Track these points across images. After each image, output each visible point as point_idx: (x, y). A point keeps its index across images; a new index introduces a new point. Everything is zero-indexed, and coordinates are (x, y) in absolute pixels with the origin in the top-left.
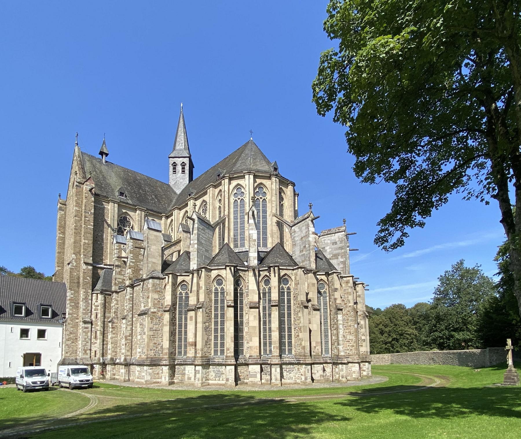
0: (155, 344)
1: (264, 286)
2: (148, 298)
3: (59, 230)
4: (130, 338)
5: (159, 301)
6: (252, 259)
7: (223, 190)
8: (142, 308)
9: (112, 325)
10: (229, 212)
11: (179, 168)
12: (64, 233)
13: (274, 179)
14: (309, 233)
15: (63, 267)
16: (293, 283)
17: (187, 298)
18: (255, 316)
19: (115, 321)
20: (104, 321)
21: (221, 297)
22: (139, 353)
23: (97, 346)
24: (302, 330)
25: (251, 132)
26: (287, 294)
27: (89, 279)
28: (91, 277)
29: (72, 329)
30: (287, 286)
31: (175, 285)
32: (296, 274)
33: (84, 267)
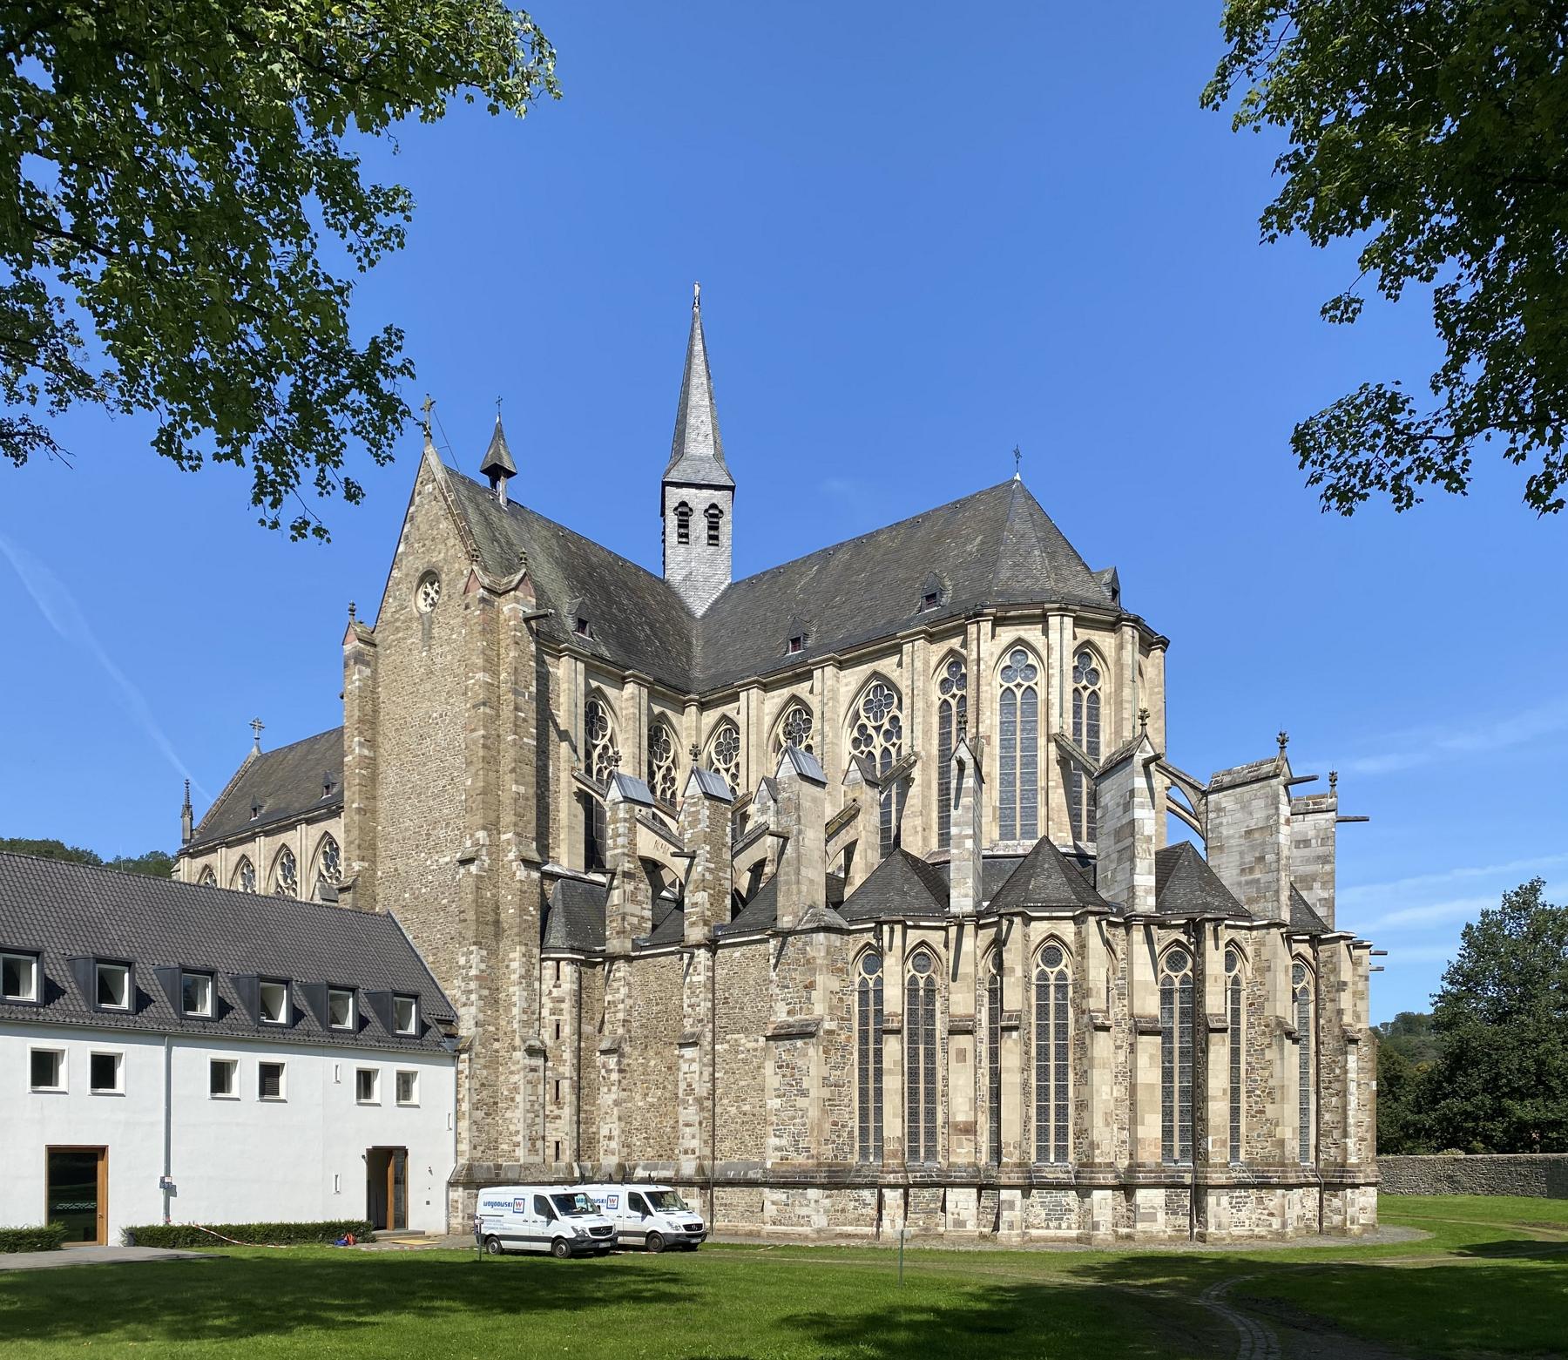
0: (835, 1124)
2: (810, 987)
3: (361, 733)
4: (708, 1104)
6: (1140, 892)
9: (619, 1063)
11: (699, 525)
12: (371, 743)
13: (1128, 632)
15: (374, 862)
16: (1249, 967)
18: (1151, 1057)
19: (627, 1049)
20: (579, 1049)
23: (562, 1129)
24: (1278, 1097)
25: (1017, 454)
29: (485, 1072)
32: (1260, 943)
33: (521, 873)
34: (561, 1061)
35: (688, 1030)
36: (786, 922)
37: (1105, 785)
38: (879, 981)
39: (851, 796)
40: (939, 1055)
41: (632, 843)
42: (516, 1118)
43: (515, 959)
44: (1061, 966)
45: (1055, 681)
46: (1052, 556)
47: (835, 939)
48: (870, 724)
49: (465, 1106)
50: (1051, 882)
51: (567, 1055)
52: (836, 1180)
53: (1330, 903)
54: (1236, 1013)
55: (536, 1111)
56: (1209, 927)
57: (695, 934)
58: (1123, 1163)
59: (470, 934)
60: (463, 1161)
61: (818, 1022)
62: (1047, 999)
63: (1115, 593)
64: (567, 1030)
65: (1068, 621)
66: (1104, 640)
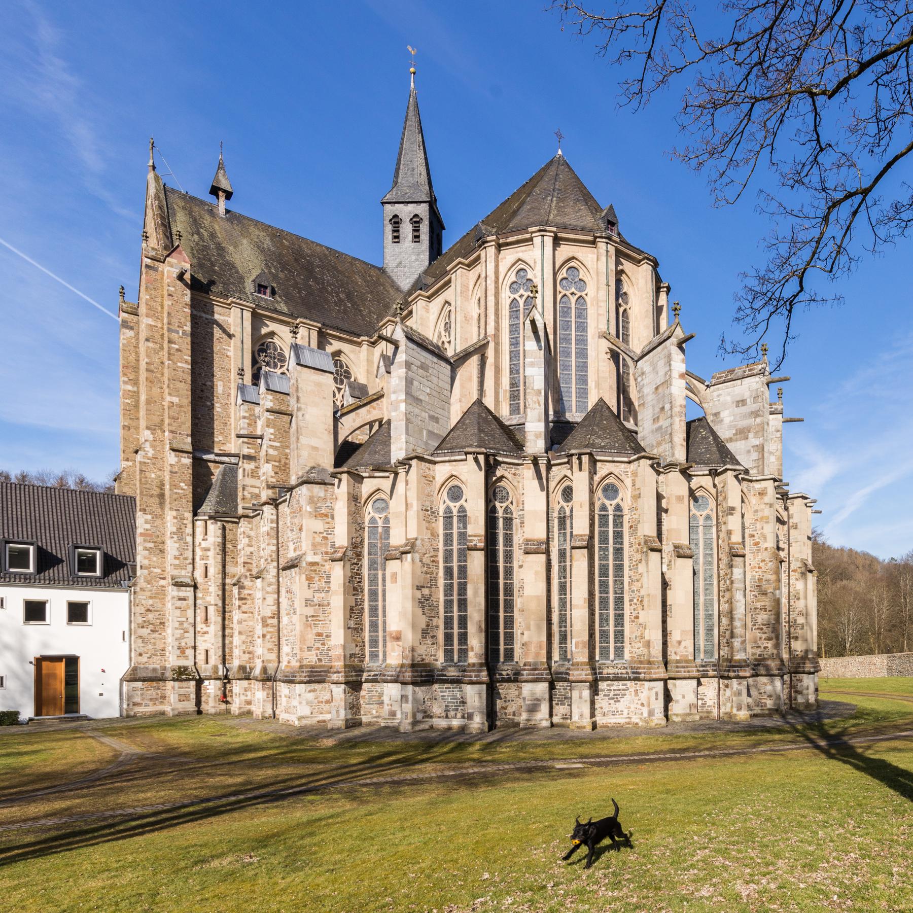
1: (562, 502)
4: (275, 621)
5: (325, 538)
7: (483, 275)
8: (292, 554)
9: (239, 593)
10: (497, 329)
14: (670, 376)
17: (387, 530)
20: (224, 585)
21: (459, 528)
22: (287, 655)
23: (209, 641)
24: (645, 603)
26: (615, 521)
27: (186, 488)
28: (190, 483)
29: (151, 602)
30: (614, 502)
31: (354, 498)
42: (170, 634)
44: (462, 502)
47: (318, 490)
62: (452, 529)
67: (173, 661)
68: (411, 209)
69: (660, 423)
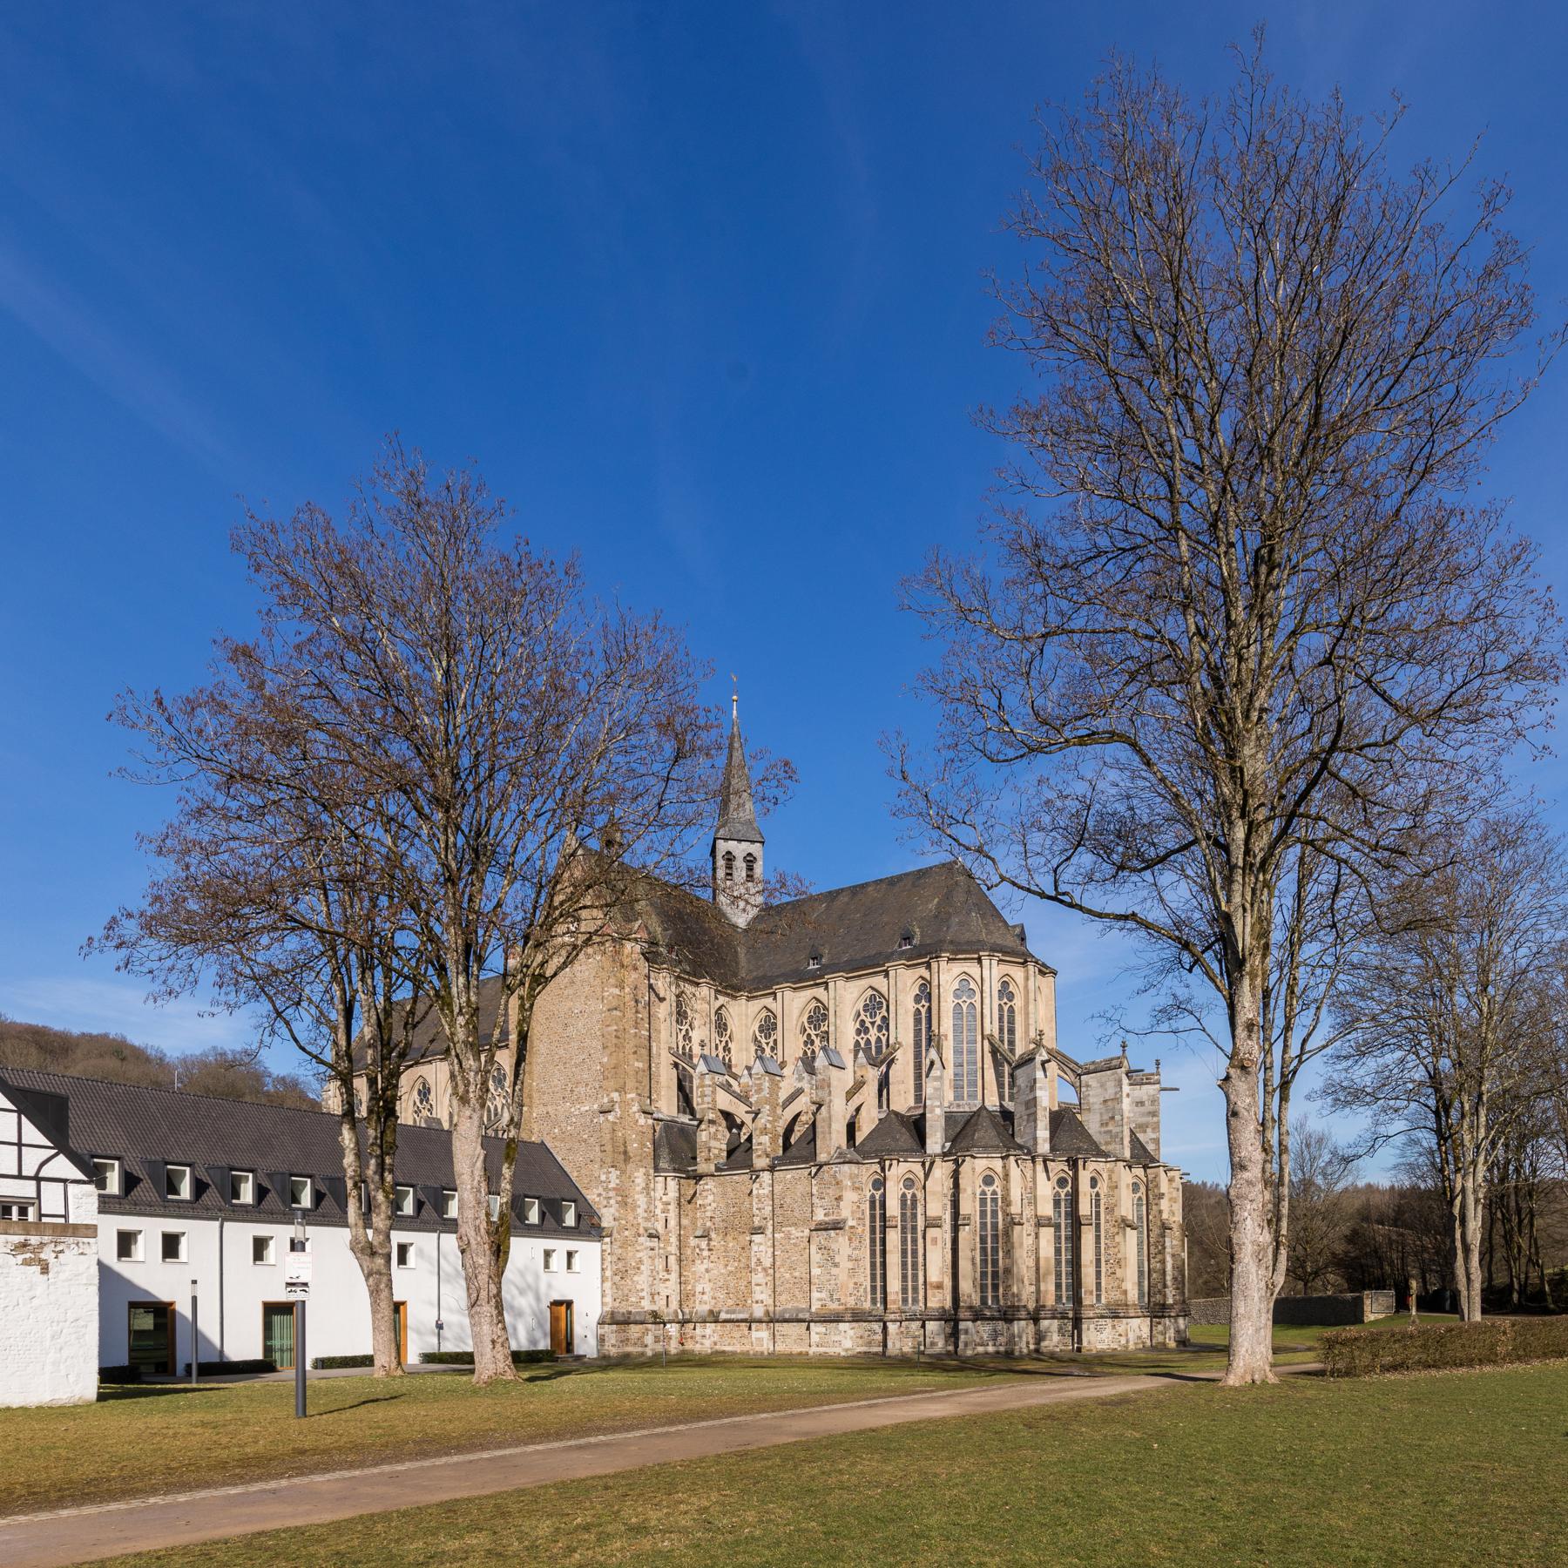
2: (839, 1199)
6: (1040, 1141)
13: (1031, 967)
19: (713, 1235)
23: (671, 1288)
32: (1111, 1171)
33: (642, 1121)
34: (668, 1242)
35: (757, 1224)
36: (822, 1157)
37: (1018, 1072)
38: (884, 1195)
39: (859, 1074)
40: (920, 1241)
41: (714, 1100)
42: (642, 1280)
43: (639, 1177)
45: (987, 1001)
46: (983, 916)
48: (868, 1020)
49: (608, 1273)
50: (986, 1133)
51: (674, 1239)
52: (858, 1317)
53: (1157, 1141)
54: (1098, 1214)
55: (653, 1274)
56: (1081, 1163)
57: (760, 1162)
58: (1031, 1306)
59: (609, 1160)
60: (607, 1309)
61: (845, 1221)
63: (1023, 939)
64: (672, 1223)
65: (994, 963)
66: (1017, 973)
67: (647, 1305)
68: (745, 847)
69: (1110, 1128)
